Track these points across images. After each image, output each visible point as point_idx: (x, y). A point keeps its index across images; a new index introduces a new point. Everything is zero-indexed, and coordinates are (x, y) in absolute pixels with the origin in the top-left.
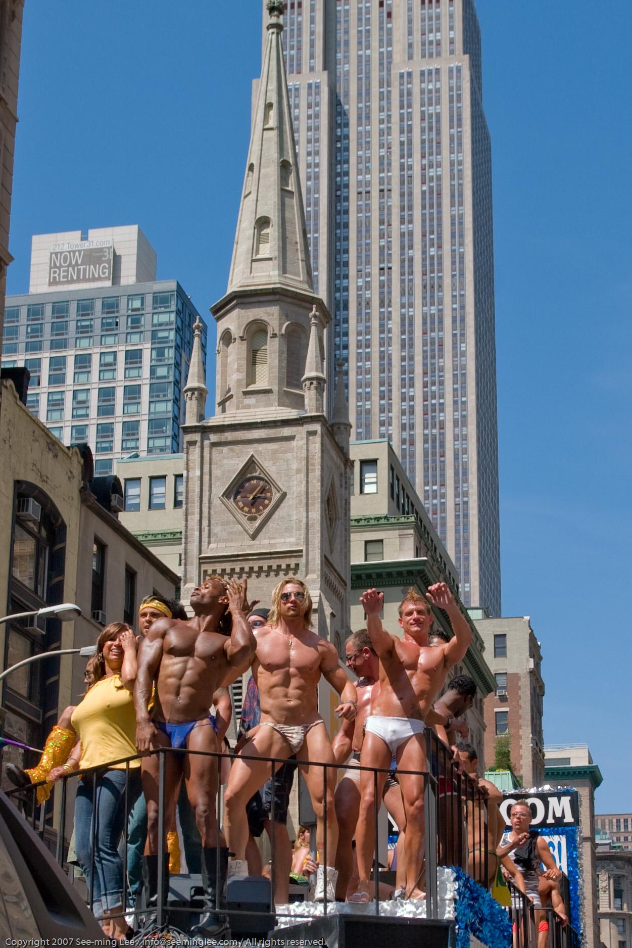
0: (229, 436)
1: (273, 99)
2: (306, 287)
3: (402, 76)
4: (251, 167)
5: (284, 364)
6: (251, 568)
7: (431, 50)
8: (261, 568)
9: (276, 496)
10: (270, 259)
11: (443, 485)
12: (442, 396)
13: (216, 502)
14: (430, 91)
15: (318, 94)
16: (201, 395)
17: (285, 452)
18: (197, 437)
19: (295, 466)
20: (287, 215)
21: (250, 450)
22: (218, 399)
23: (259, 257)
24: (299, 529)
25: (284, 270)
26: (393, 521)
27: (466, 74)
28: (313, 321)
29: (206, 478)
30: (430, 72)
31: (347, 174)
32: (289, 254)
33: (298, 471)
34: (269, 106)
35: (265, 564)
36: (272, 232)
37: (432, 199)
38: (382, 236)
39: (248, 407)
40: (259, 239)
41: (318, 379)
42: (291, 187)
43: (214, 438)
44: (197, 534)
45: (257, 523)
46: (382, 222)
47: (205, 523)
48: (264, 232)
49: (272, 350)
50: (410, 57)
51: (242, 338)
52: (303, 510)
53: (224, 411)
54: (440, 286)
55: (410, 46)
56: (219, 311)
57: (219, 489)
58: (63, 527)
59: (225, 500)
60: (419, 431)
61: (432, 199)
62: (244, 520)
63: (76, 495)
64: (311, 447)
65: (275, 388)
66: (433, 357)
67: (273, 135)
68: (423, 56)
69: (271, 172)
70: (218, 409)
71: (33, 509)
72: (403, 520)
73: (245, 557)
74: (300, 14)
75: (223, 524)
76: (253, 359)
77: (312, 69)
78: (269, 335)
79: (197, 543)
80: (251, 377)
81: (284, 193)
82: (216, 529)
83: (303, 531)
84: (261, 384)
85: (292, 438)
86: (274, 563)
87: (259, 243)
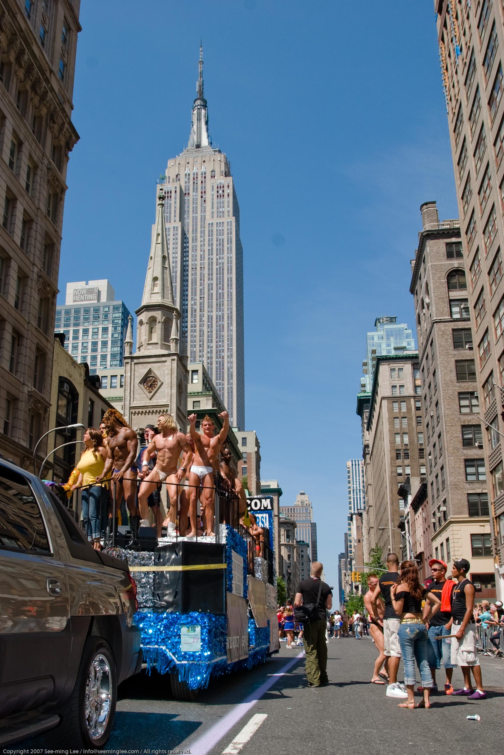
0: (141, 360)
1: (160, 232)
2: (172, 304)
3: (209, 224)
4: (151, 258)
5: (163, 333)
6: (149, 411)
7: (221, 214)
8: (153, 411)
9: (159, 384)
10: (158, 293)
11: (223, 380)
12: (223, 346)
13: (136, 385)
14: (220, 230)
15: (177, 230)
16: (131, 344)
17: (163, 367)
18: (129, 361)
19: (166, 372)
20: (165, 276)
21: (149, 366)
22: (137, 346)
23: (154, 292)
24: (168, 396)
25: (163, 297)
26: (204, 394)
27: (234, 224)
28: (174, 317)
29: (132, 376)
30: (220, 223)
31: (188, 261)
32: (165, 291)
33: (168, 374)
34: (158, 235)
35: (155, 410)
36: (159, 282)
37: (220, 271)
38: (201, 285)
39: (149, 349)
40: (154, 285)
41: (176, 339)
42: (167, 266)
43: (136, 361)
44: (129, 398)
45: (152, 394)
46: (201, 280)
47: (132, 393)
48: (156, 282)
49: (158, 328)
50: (213, 217)
51: (147, 323)
52: (169, 389)
53: (139, 351)
54: (223, 304)
55: (213, 213)
56: (138, 312)
57: (138, 380)
58: (77, 394)
59: (140, 385)
60: (214, 359)
61: (220, 271)
62: (147, 393)
63: (82, 382)
64: (173, 364)
65: (159, 342)
66: (220, 331)
67: (160, 246)
68: (218, 217)
69: (159, 260)
70: (137, 350)
71: (66, 387)
72: (208, 393)
73: (147, 407)
74: (170, 200)
75: (139, 394)
76: (151, 332)
77: (175, 221)
78: (157, 322)
79: (129, 401)
80: (150, 338)
81: (164, 268)
82: (136, 396)
83: (170, 397)
84: (154, 340)
85: (165, 362)
86: (158, 409)
87: (154, 286)
